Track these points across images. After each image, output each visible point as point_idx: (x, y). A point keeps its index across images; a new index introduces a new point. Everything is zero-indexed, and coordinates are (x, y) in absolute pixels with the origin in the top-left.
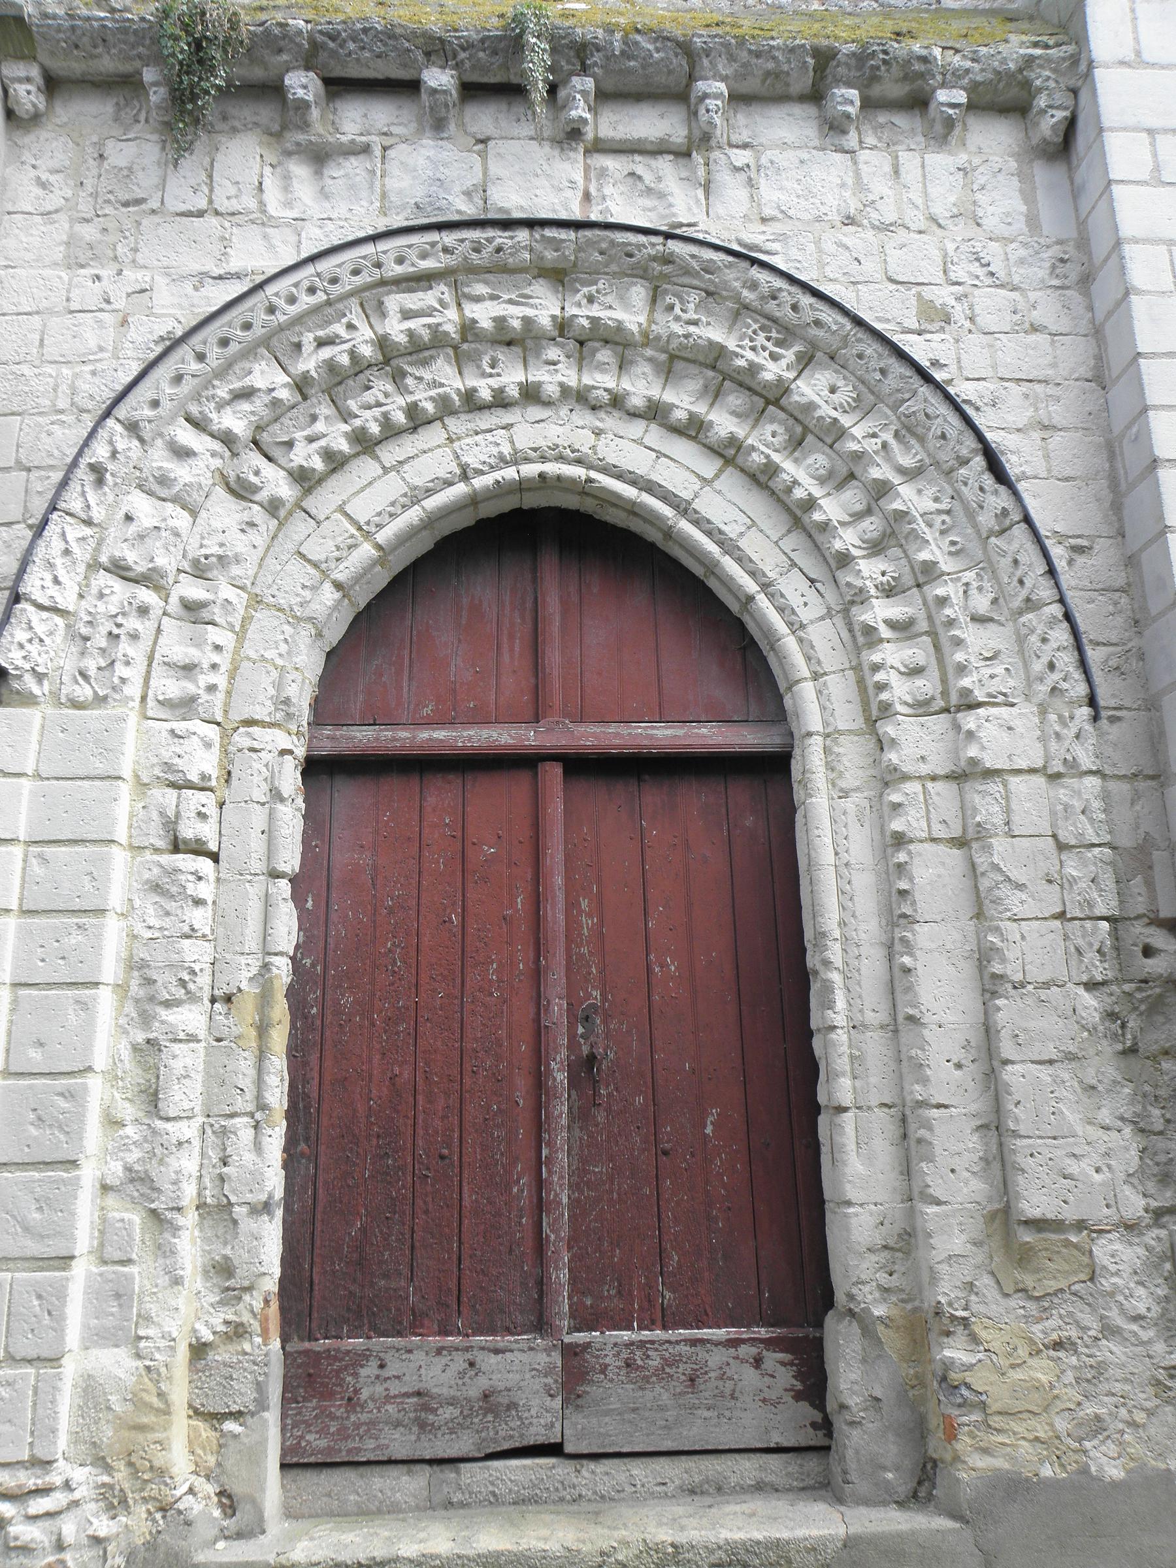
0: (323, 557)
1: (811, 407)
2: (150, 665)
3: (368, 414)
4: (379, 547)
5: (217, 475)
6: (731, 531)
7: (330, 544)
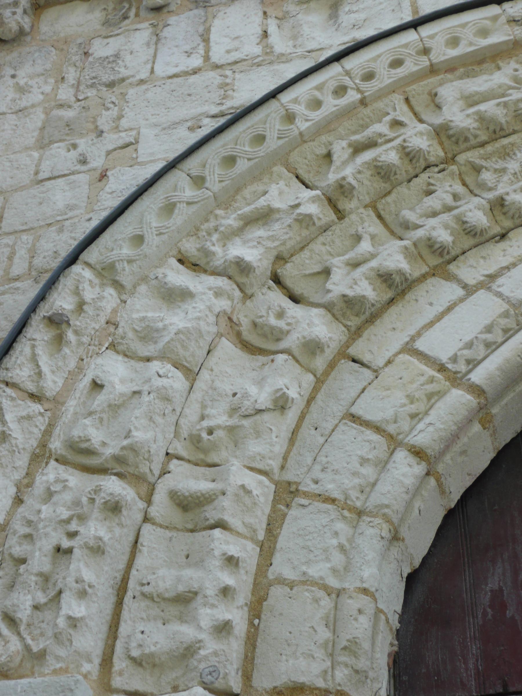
0: (389, 414)
2: (119, 604)
3: (432, 222)
4: (477, 390)
5: (223, 321)
7: (398, 397)
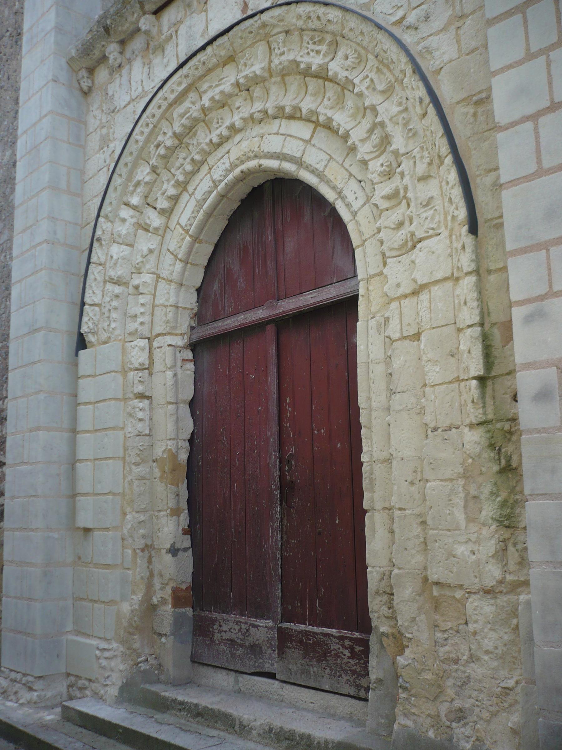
1: (336, 74)
6: (320, 167)
